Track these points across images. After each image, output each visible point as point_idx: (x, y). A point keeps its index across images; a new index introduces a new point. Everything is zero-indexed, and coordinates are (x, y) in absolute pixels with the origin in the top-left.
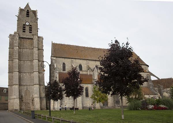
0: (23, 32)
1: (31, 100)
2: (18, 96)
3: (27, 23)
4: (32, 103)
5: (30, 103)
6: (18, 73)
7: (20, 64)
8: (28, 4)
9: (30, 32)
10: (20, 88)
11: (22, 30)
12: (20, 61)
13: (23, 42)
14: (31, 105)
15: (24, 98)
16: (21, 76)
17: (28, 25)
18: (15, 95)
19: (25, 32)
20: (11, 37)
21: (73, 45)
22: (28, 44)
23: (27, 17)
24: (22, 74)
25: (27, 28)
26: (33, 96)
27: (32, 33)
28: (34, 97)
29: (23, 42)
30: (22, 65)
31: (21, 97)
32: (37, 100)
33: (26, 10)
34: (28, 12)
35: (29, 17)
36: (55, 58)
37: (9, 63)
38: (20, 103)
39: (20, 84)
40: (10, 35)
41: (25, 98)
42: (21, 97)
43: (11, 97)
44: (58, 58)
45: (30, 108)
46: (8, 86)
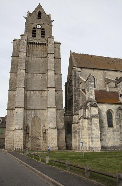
0: (33, 36)
1: (42, 134)
2: (22, 126)
3: (38, 26)
4: (44, 138)
6: (23, 89)
7: (26, 77)
8: (40, 4)
9: (42, 37)
10: (25, 113)
11: (32, 34)
12: (26, 73)
13: (32, 49)
14: (41, 141)
15: (30, 129)
16: (28, 96)
17: (40, 28)
18: (16, 124)
19: (35, 36)
20: (16, 42)
21: (99, 55)
22: (39, 51)
24: (29, 92)
25: (38, 33)
26: (44, 126)
27: (45, 38)
28: (46, 128)
29: (32, 49)
30: (30, 79)
31: (26, 128)
32: (52, 134)
33: (38, 12)
36: (79, 69)
37: (10, 76)
38: (25, 137)
39: (25, 107)
40: (15, 40)
41: (32, 130)
42: (25, 129)
43: (11, 128)
44: (83, 70)
45: (40, 145)
46: (7, 110)
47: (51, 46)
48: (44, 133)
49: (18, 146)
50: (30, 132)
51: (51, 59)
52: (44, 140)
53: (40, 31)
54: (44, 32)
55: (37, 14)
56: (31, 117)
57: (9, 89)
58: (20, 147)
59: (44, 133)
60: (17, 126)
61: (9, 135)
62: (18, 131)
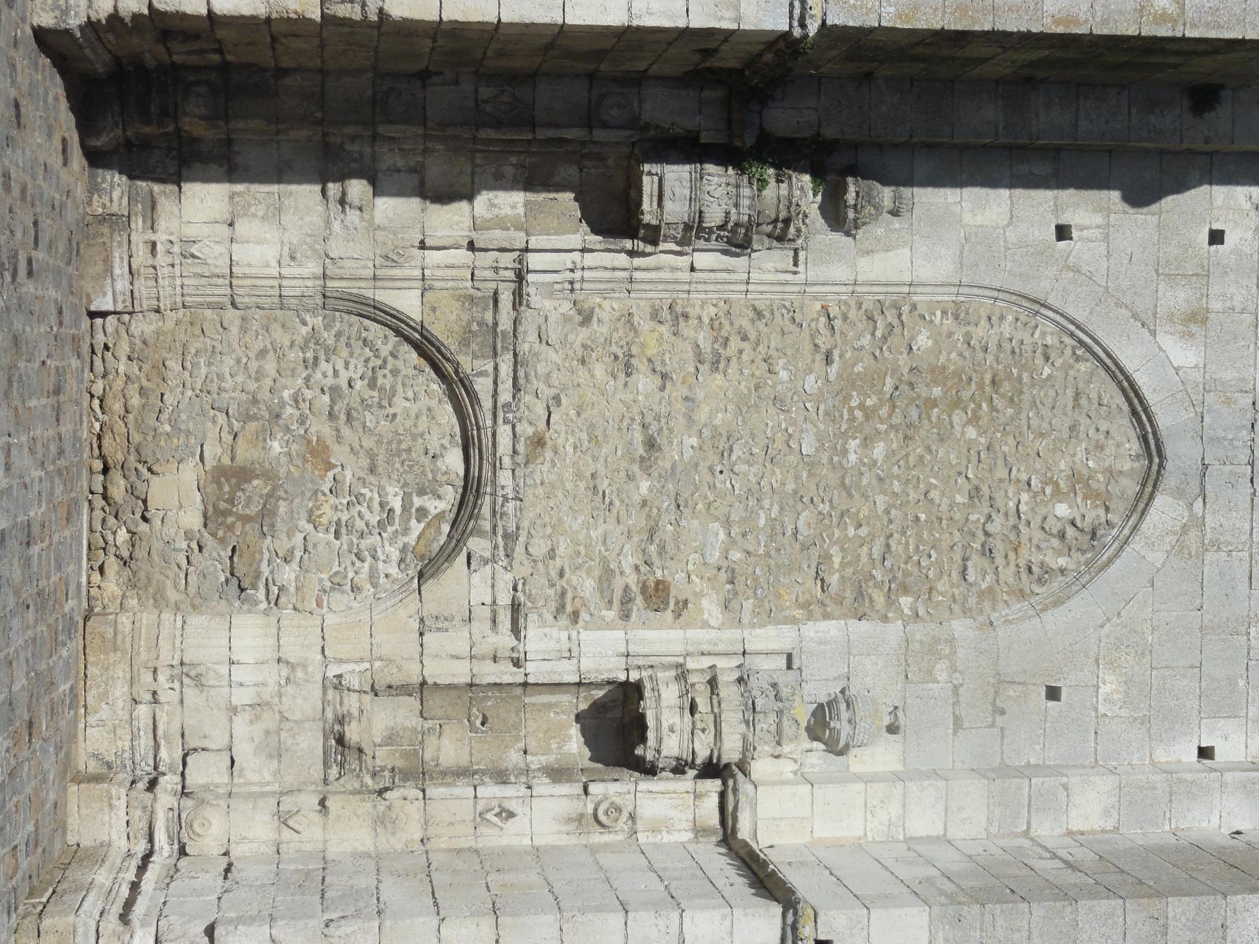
52: (403, 713)
56: (1147, 323)
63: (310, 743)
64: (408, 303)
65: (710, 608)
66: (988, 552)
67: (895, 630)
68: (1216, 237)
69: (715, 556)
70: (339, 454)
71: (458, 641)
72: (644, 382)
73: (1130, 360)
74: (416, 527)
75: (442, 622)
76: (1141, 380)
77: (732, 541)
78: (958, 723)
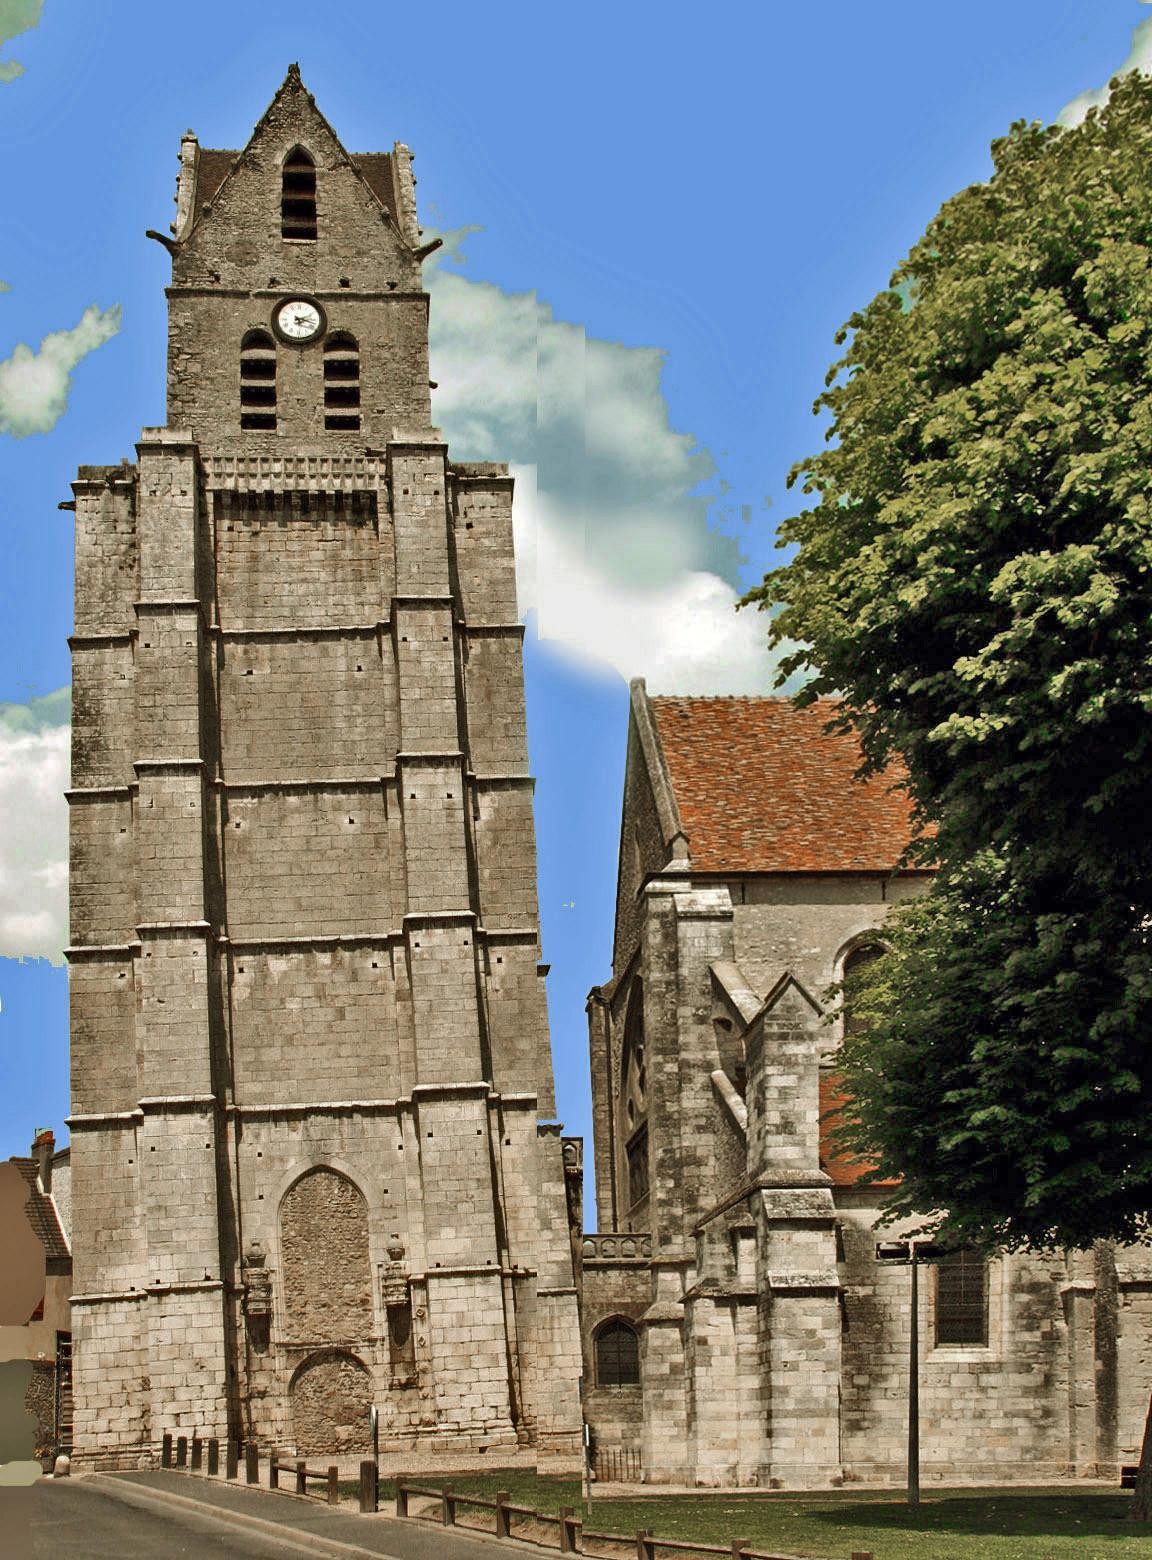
0: (248, 422)
1: (380, 1317)
5: (364, 1354)
8: (293, 82)
9: (332, 423)
11: (236, 403)
15: (277, 1280)
17: (305, 332)
18: (160, 1240)
23: (287, 232)
27: (364, 430)
33: (279, 159)
34: (299, 181)
35: (311, 234)
37: (74, 823)
43: (117, 1273)
47: (423, 524)
48: (400, 1318)
49: (183, 1419)
50: (278, 1306)
51: (428, 659)
53: (314, 363)
54: (350, 369)
55: (278, 184)
57: (74, 943)
58: (205, 1433)
59: (400, 1318)
60: (166, 1261)
61: (102, 1332)
62: (173, 1297)
63: (409, 1393)
64: (290, 1373)
65: (367, 1288)
66: (349, 1212)
67: (372, 1237)
68: (260, 1155)
69: (353, 1287)
70: (331, 1389)
71: (378, 1355)
72: (309, 1308)
73: (294, 1177)
74: (350, 1367)
75: (374, 1359)
76: (300, 1172)
77: (349, 1283)
78: (395, 1217)
